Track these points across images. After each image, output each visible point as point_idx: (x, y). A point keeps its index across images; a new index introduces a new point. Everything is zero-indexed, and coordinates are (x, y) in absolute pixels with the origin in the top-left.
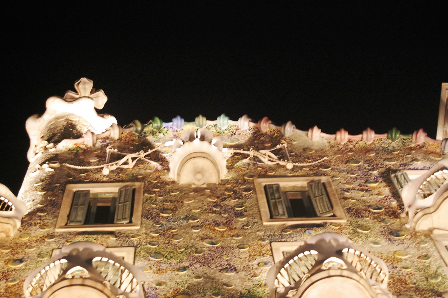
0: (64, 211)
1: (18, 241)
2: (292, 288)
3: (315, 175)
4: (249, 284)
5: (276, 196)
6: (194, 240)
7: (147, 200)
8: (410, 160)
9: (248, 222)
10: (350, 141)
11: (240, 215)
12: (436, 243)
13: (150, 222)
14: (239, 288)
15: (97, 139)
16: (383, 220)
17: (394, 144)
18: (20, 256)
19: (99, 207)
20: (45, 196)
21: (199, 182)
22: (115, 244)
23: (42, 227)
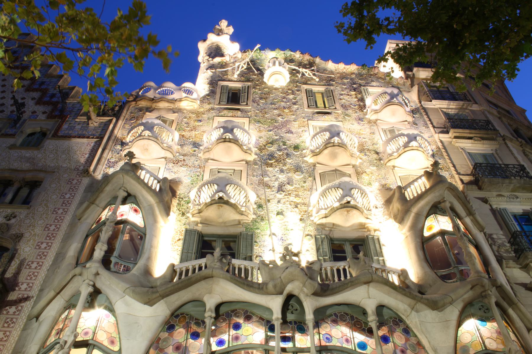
0: (218, 96)
3: (328, 85)
4: (298, 141)
9: (298, 108)
11: (294, 104)
13: (255, 105)
14: (294, 143)
17: (364, 72)
18: (200, 119)
19: (232, 93)
21: (277, 85)
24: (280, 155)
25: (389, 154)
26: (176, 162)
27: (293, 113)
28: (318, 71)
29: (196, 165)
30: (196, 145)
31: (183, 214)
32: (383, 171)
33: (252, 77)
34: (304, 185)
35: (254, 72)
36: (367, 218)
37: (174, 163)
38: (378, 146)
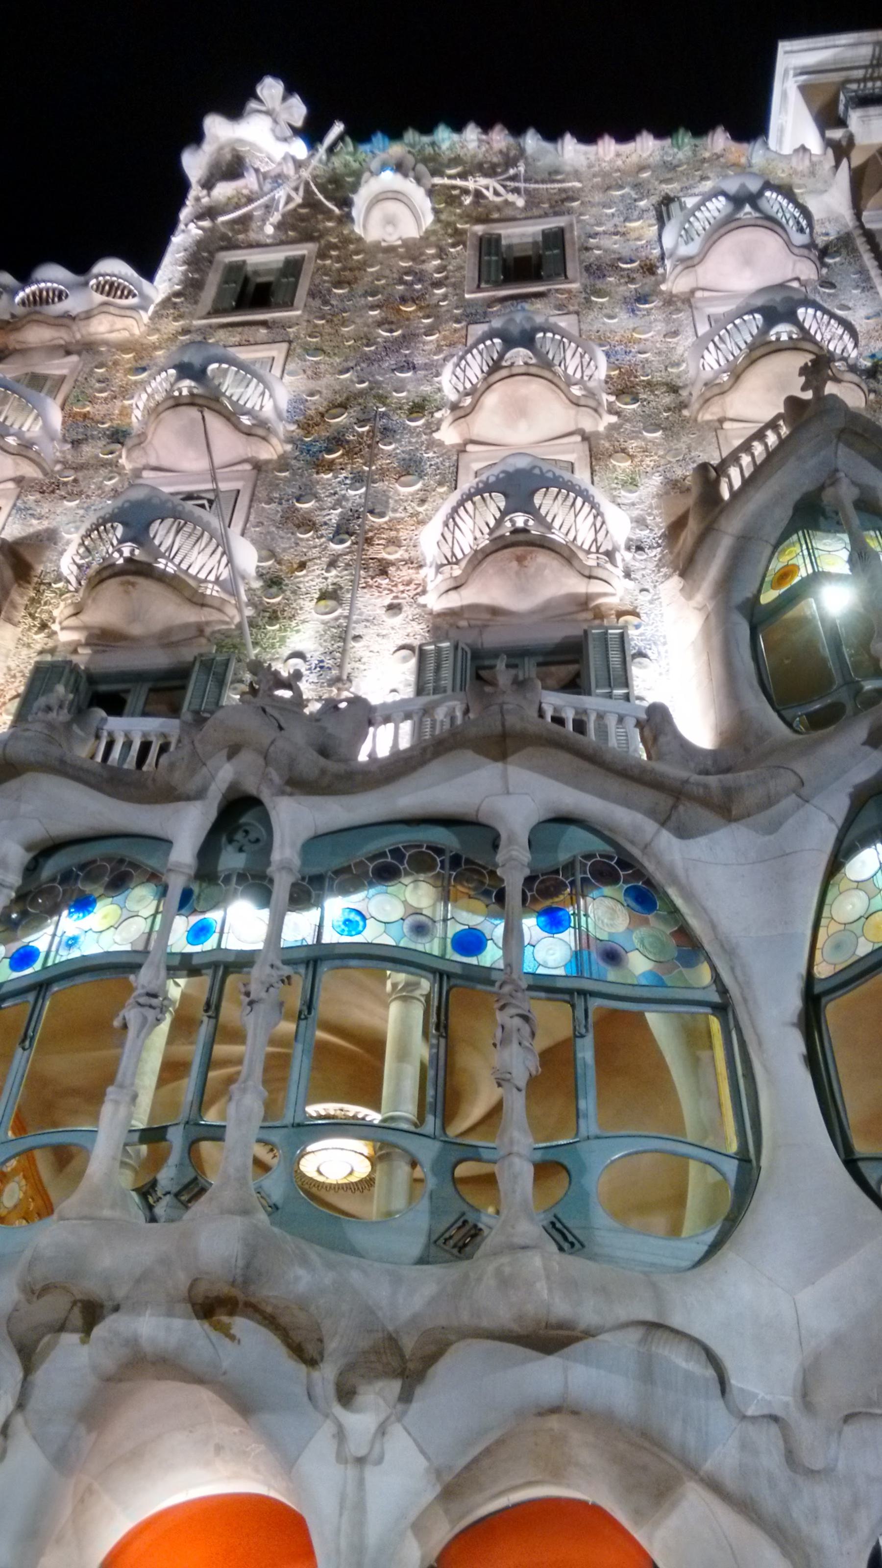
0: (209, 295)
1: (145, 341)
2: (467, 394)
4: (426, 389)
5: (493, 251)
6: (369, 326)
7: (318, 270)
8: (698, 179)
10: (618, 155)
11: (438, 284)
12: (695, 313)
13: (317, 302)
15: (265, 178)
16: (632, 280)
18: (144, 363)
20: (185, 273)
21: (392, 237)
22: (265, 340)
23: (175, 319)
24: (360, 435)
25: (706, 384)
26: (50, 488)
27: (427, 311)
28: (527, 180)
29: (107, 489)
30: (118, 436)
31: (44, 626)
32: (684, 439)
33: (320, 226)
34: (420, 509)
35: (330, 211)
36: (590, 577)
37: (43, 492)
38: (683, 367)
